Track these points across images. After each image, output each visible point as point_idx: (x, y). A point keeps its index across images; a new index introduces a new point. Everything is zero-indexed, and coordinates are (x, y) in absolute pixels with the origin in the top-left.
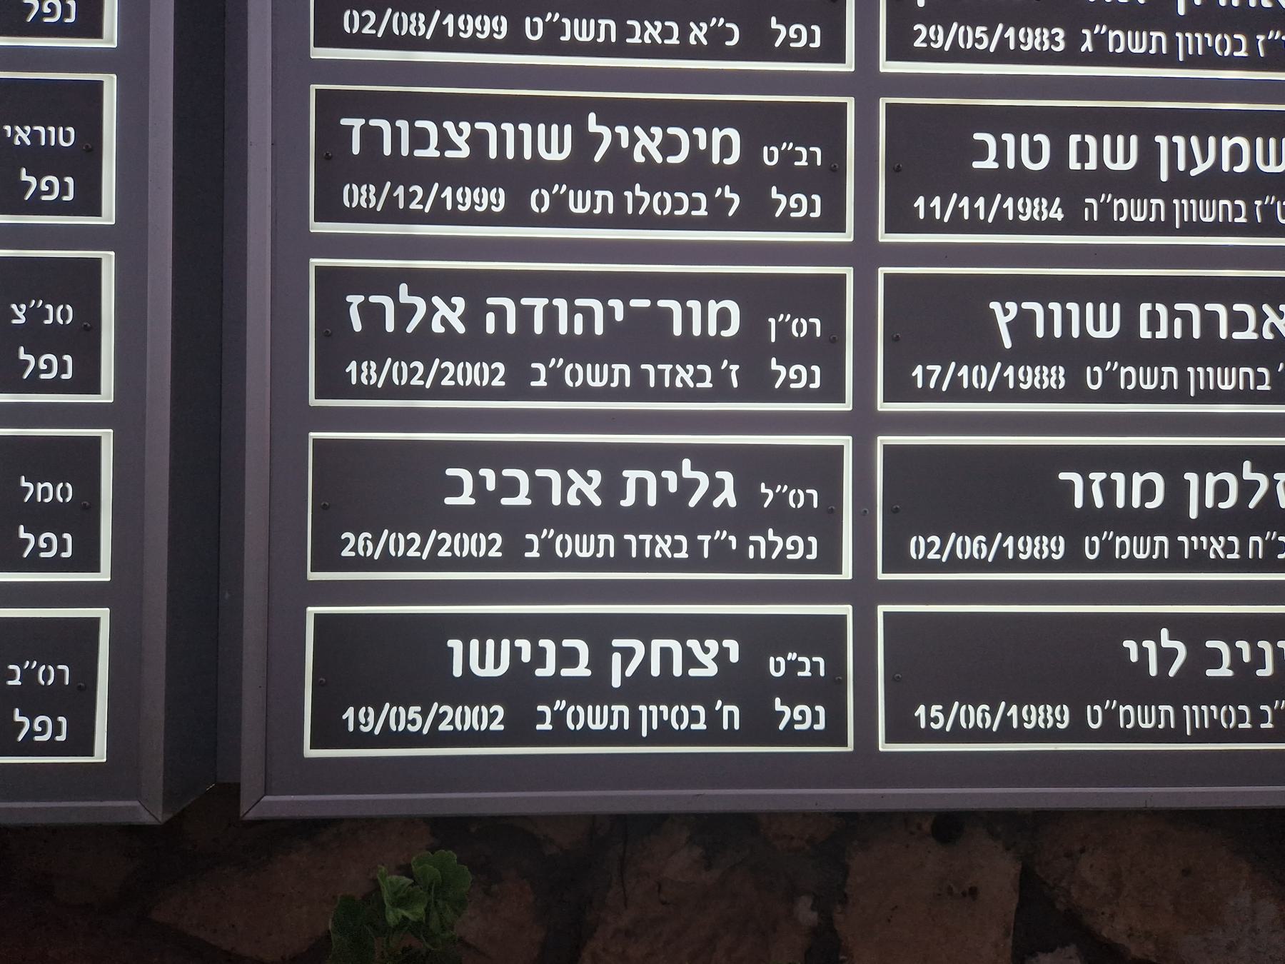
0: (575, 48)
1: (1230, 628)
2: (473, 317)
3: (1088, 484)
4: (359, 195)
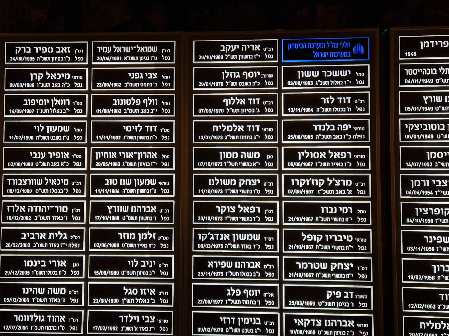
2: (26, 209)
3: (123, 235)
4: (9, 191)
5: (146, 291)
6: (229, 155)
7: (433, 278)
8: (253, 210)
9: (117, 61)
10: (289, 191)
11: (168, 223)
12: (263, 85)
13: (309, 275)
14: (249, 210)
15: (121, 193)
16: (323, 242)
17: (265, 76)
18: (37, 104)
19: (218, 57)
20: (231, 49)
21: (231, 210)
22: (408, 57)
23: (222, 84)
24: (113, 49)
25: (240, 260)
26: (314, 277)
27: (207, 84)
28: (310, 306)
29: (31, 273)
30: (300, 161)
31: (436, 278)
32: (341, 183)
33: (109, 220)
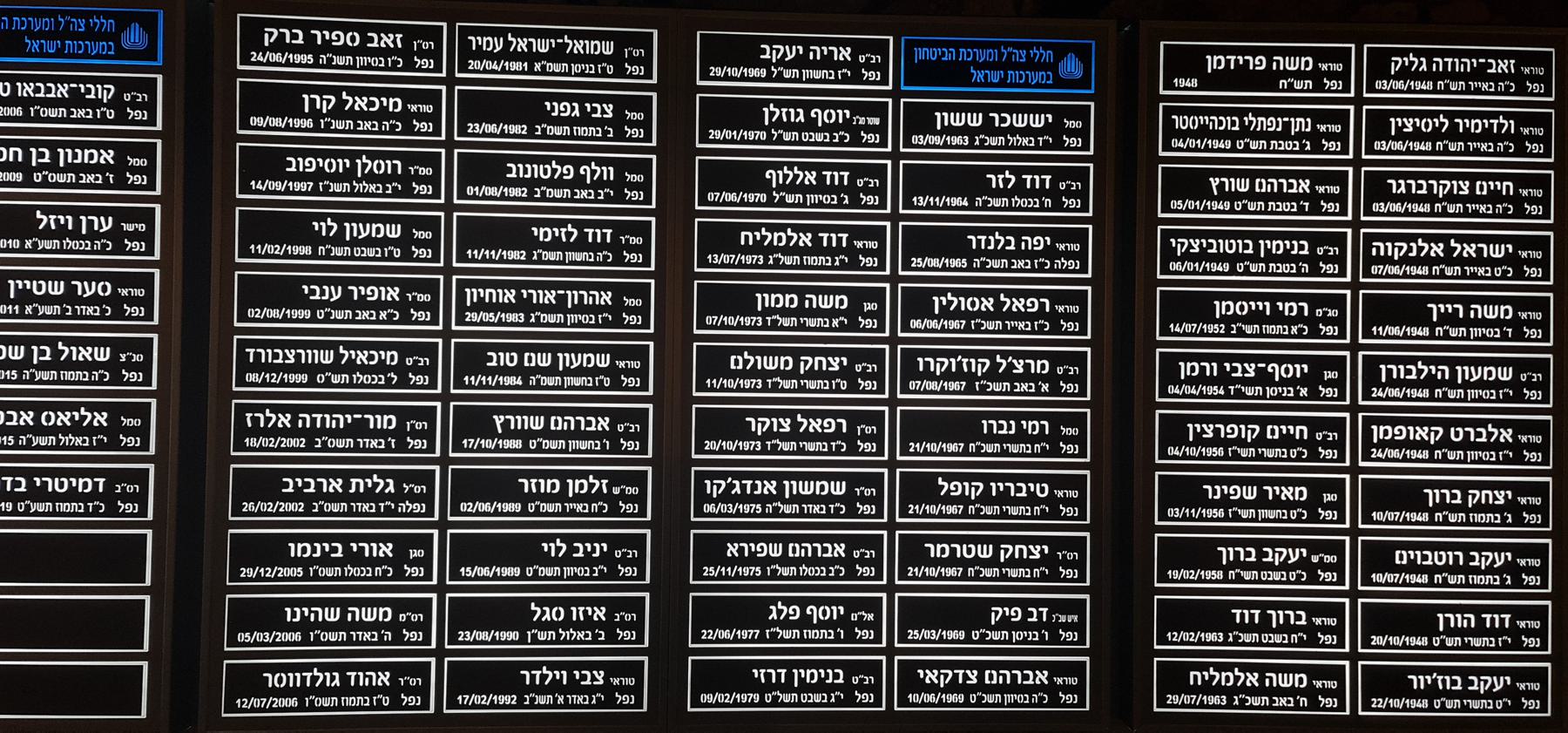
0: (336, 321)
1: (583, 539)
2: (294, 421)
4: (252, 377)
5: (585, 612)
6: (777, 301)
7: (1219, 575)
8: (830, 425)
9: (516, 72)
10: (912, 385)
11: (640, 457)
12: (857, 141)
13: (951, 572)
14: (822, 427)
15: (526, 386)
16: (986, 498)
17: (862, 121)
18: (320, 170)
19: (754, 72)
20: (785, 55)
21: (780, 426)
22: (1179, 89)
23: (763, 135)
24: (507, 44)
25: (800, 539)
26: (964, 577)
27: (728, 134)
28: (953, 641)
29: (306, 571)
30: (938, 318)
31: (1226, 575)
32: (1027, 367)
33: (497, 449)
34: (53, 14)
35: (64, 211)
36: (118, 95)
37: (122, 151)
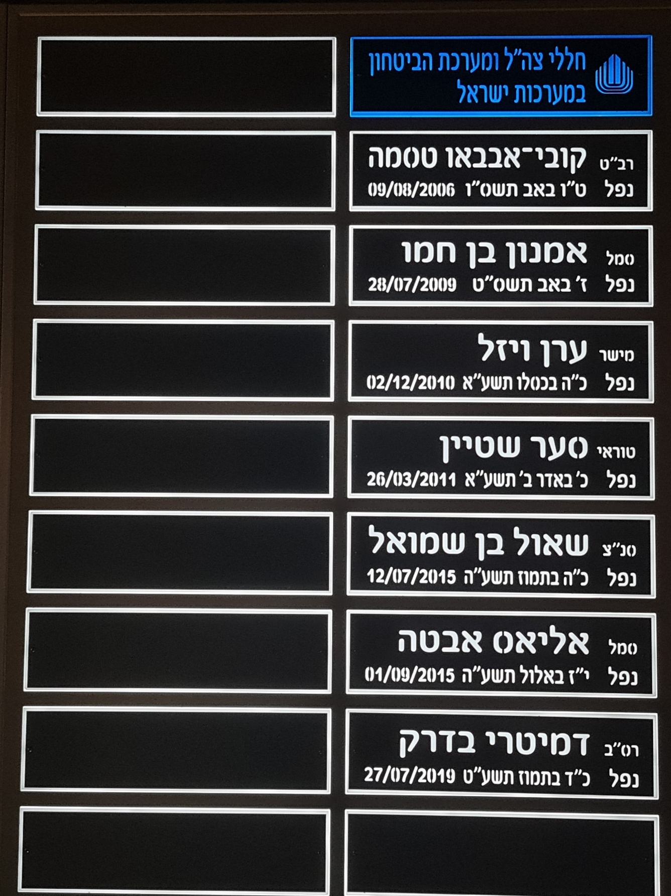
34: (495, 47)
35: (518, 333)
36: (592, 162)
37: (599, 244)
